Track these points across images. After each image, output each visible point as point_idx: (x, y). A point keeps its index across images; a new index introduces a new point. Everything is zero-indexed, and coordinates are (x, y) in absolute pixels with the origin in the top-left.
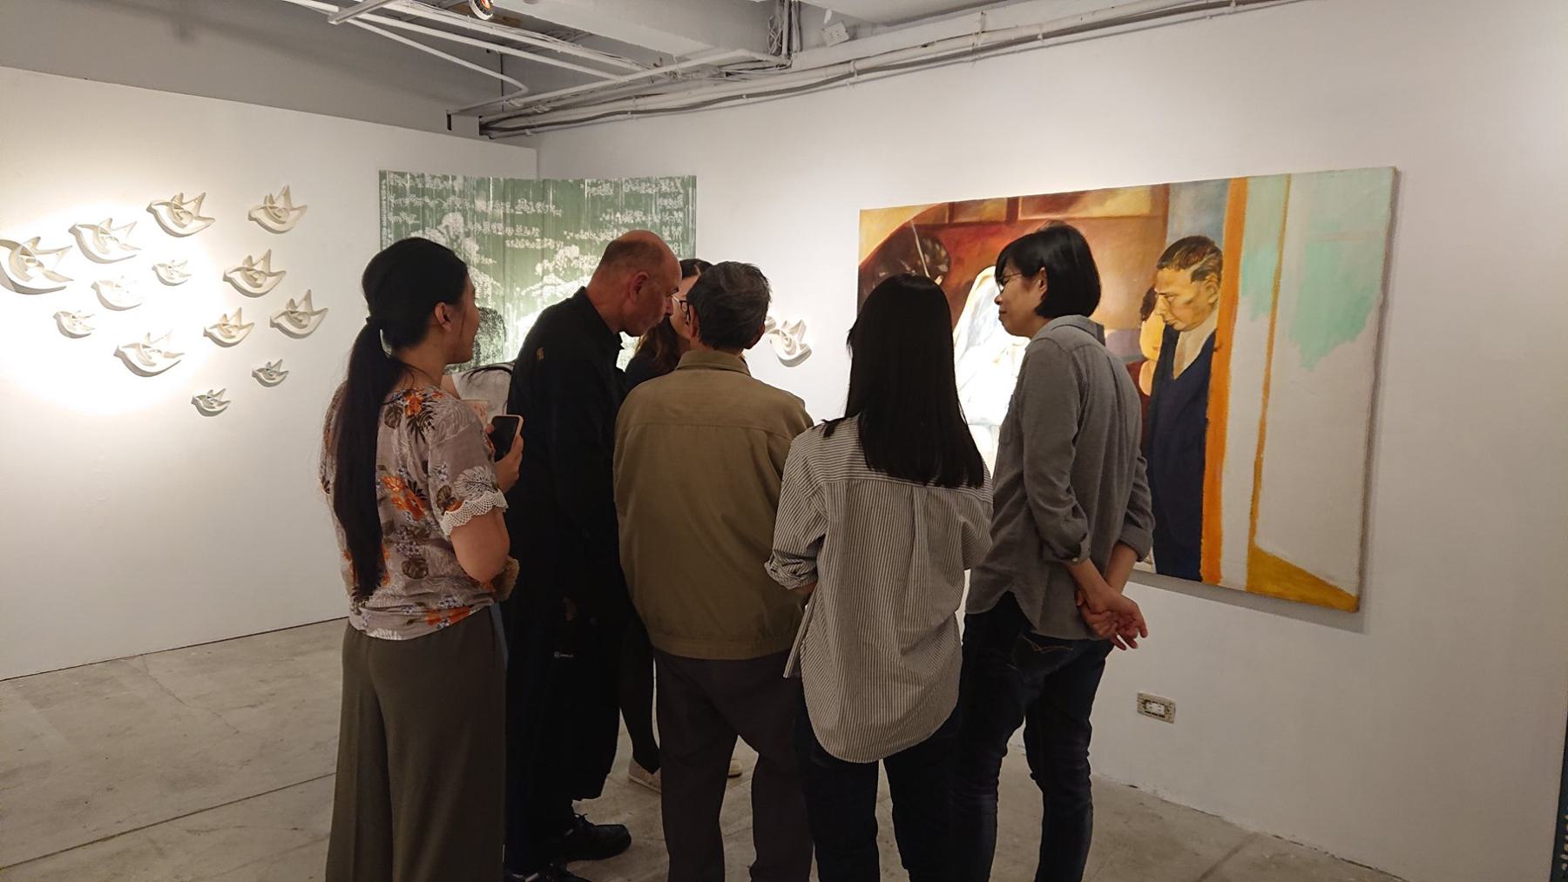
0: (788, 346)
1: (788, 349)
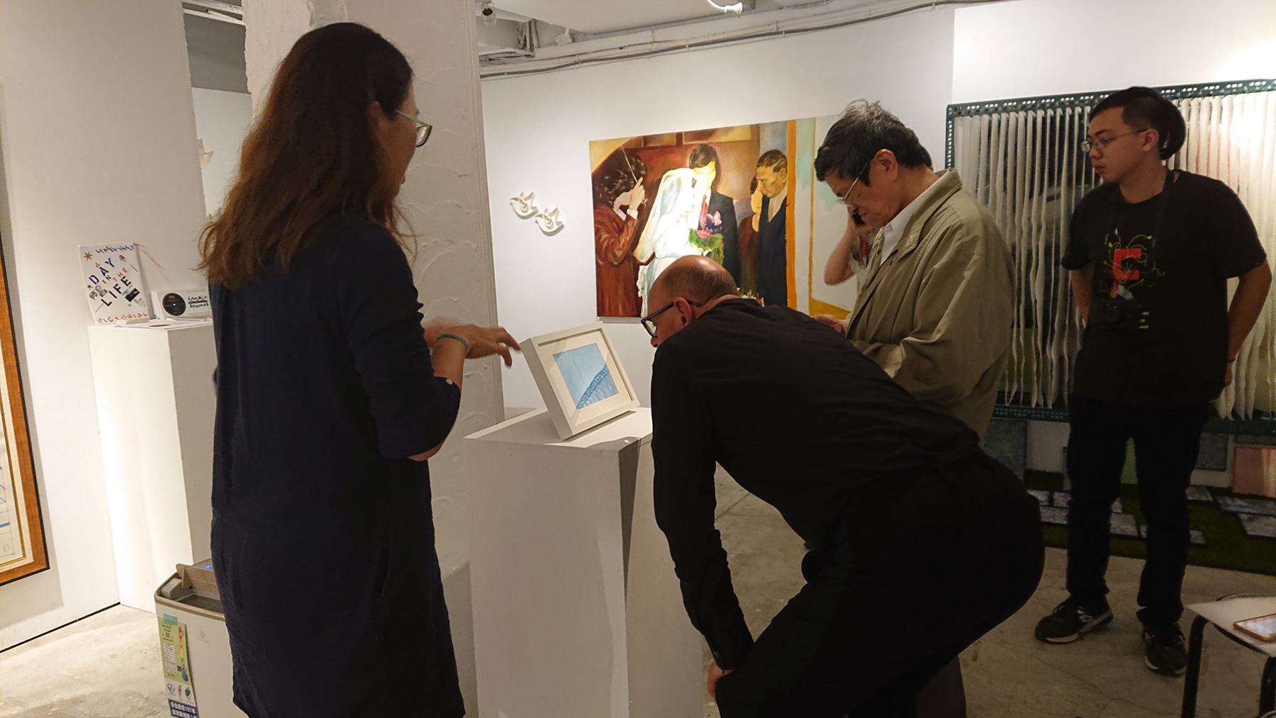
0: (549, 224)
1: (548, 225)
